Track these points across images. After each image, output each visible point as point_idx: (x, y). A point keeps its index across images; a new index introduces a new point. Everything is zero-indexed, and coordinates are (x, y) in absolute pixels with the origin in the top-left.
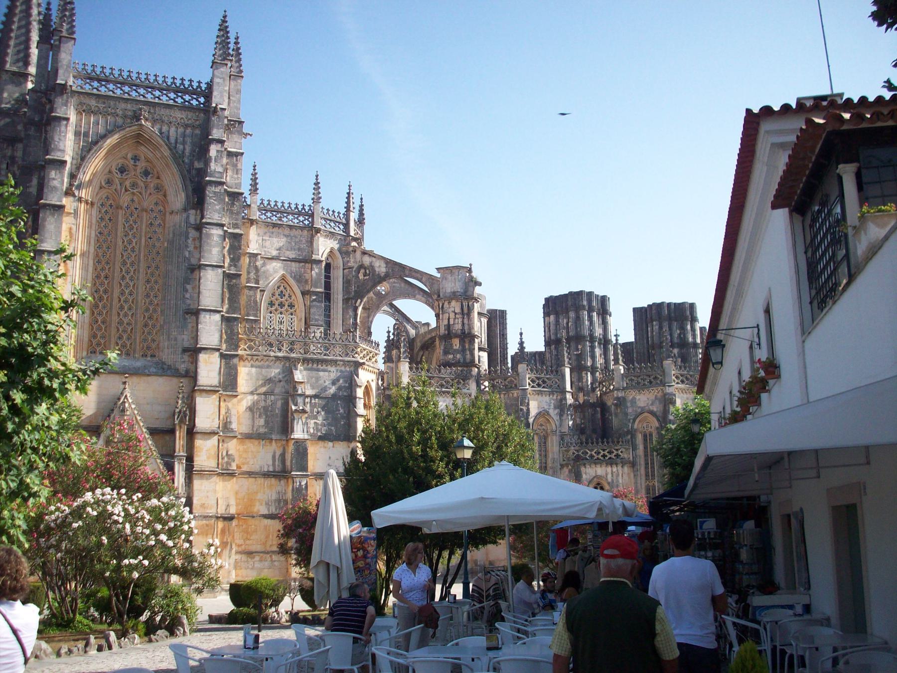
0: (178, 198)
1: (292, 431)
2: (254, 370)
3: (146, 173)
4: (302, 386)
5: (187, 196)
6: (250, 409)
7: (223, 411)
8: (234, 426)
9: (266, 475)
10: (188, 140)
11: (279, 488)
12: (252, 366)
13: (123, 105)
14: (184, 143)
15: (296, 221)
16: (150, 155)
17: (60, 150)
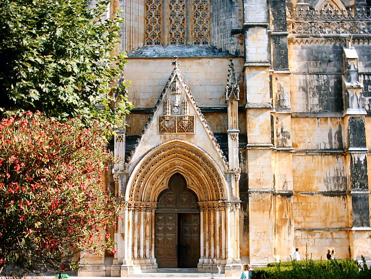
8: (287, 103)
9: (324, 152)
11: (337, 166)
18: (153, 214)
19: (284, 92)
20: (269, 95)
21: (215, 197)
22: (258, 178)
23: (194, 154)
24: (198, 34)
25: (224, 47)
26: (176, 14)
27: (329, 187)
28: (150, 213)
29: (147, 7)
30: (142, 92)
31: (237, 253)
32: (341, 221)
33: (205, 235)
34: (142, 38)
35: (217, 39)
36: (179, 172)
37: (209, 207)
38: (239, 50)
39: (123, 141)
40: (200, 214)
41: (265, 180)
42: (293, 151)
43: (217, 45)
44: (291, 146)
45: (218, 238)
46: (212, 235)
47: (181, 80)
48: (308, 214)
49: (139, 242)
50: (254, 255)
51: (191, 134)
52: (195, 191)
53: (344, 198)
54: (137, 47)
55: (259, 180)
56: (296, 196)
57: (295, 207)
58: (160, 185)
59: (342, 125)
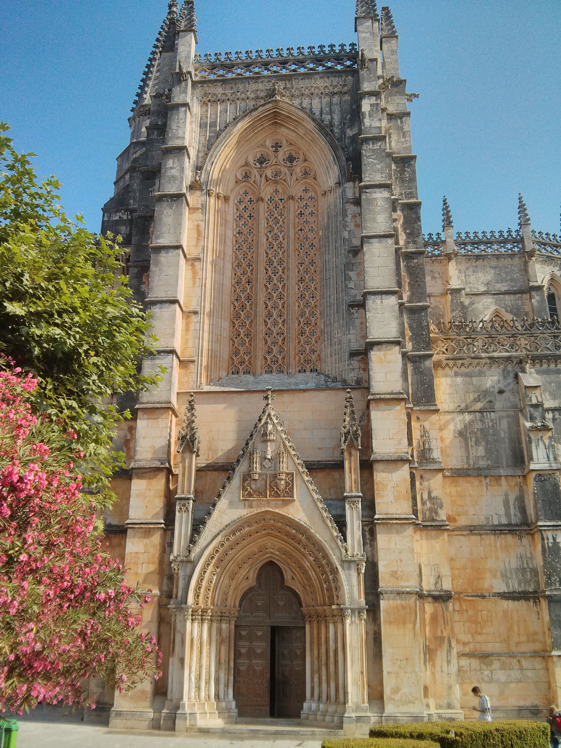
0: (328, 173)
1: (531, 459)
2: (459, 380)
3: (291, 159)
4: (537, 392)
5: (341, 168)
6: (461, 434)
7: (416, 435)
8: (436, 454)
9: (498, 530)
10: (336, 109)
11: (521, 550)
12: (456, 374)
13: (253, 86)
14: (331, 113)
15: (503, 250)
16: (292, 136)
17: (178, 138)
18: (233, 627)
19: (431, 437)
20: (406, 442)
21: (327, 599)
22: (394, 569)
23: (294, 531)
24: (304, 357)
26: (273, 332)
29: (234, 323)
34: (225, 365)
35: (329, 365)
37: (318, 617)
40: (304, 628)
42: (448, 527)
43: (330, 373)
44: (445, 519)
45: (332, 667)
46: (323, 663)
47: (276, 421)
48: (479, 630)
52: (297, 591)
53: (535, 602)
55: (396, 572)
56: (459, 599)
57: (457, 617)
58: (244, 581)
59: (525, 487)
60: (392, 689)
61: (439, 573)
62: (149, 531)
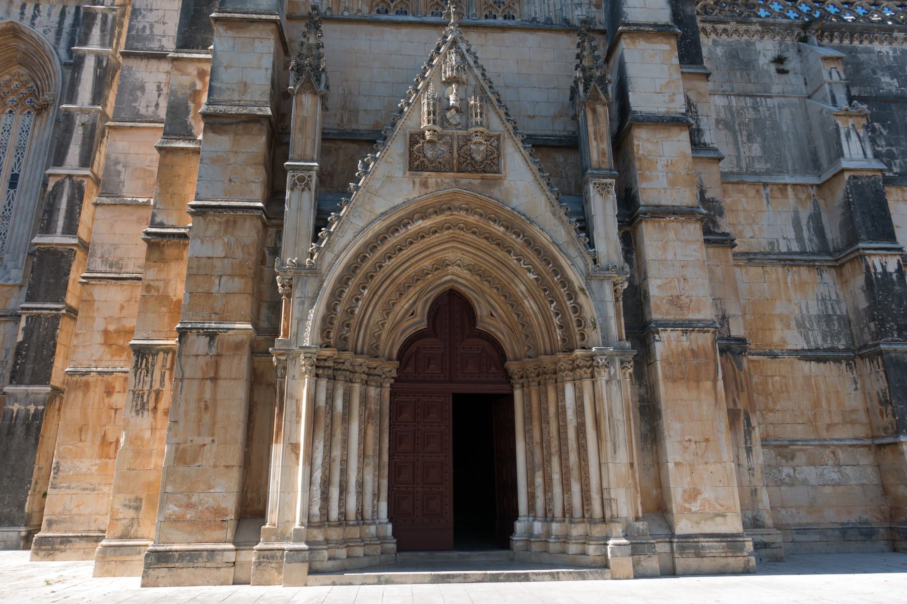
9: (788, 261)
11: (822, 290)
23: (502, 229)
25: (555, 16)
27: (812, 339)
28: (378, 390)
30: (365, 96)
31: (636, 504)
32: (853, 423)
33: (530, 454)
36: (456, 285)
38: (594, 18)
39: (310, 189)
40: (511, 397)
41: (694, 298)
43: (537, 16)
45: (573, 458)
48: (771, 405)
49: (344, 472)
50: (686, 509)
51: (494, 179)
52: (499, 334)
53: (848, 364)
54: (355, 8)
55: (678, 297)
60: (685, 491)
61: (724, 311)
62: (235, 222)
